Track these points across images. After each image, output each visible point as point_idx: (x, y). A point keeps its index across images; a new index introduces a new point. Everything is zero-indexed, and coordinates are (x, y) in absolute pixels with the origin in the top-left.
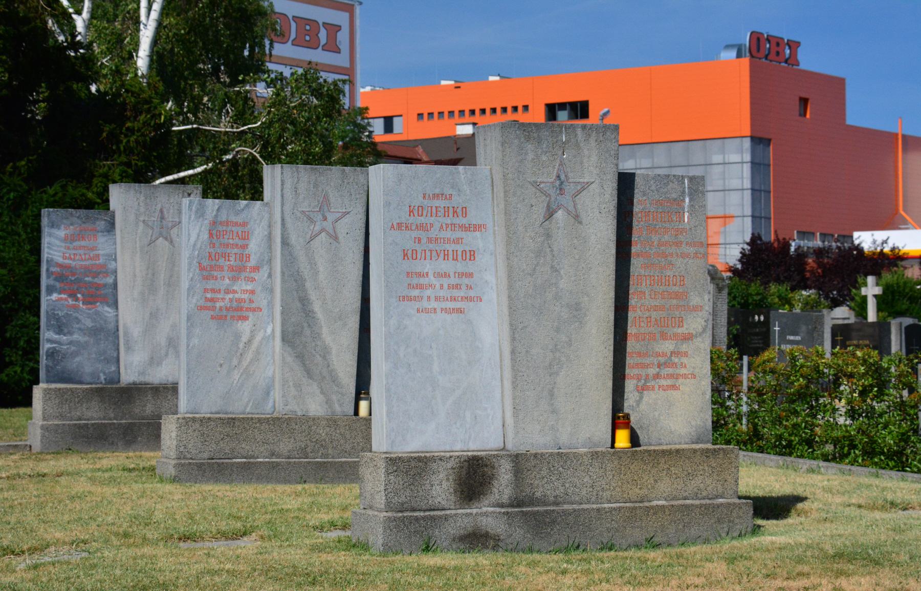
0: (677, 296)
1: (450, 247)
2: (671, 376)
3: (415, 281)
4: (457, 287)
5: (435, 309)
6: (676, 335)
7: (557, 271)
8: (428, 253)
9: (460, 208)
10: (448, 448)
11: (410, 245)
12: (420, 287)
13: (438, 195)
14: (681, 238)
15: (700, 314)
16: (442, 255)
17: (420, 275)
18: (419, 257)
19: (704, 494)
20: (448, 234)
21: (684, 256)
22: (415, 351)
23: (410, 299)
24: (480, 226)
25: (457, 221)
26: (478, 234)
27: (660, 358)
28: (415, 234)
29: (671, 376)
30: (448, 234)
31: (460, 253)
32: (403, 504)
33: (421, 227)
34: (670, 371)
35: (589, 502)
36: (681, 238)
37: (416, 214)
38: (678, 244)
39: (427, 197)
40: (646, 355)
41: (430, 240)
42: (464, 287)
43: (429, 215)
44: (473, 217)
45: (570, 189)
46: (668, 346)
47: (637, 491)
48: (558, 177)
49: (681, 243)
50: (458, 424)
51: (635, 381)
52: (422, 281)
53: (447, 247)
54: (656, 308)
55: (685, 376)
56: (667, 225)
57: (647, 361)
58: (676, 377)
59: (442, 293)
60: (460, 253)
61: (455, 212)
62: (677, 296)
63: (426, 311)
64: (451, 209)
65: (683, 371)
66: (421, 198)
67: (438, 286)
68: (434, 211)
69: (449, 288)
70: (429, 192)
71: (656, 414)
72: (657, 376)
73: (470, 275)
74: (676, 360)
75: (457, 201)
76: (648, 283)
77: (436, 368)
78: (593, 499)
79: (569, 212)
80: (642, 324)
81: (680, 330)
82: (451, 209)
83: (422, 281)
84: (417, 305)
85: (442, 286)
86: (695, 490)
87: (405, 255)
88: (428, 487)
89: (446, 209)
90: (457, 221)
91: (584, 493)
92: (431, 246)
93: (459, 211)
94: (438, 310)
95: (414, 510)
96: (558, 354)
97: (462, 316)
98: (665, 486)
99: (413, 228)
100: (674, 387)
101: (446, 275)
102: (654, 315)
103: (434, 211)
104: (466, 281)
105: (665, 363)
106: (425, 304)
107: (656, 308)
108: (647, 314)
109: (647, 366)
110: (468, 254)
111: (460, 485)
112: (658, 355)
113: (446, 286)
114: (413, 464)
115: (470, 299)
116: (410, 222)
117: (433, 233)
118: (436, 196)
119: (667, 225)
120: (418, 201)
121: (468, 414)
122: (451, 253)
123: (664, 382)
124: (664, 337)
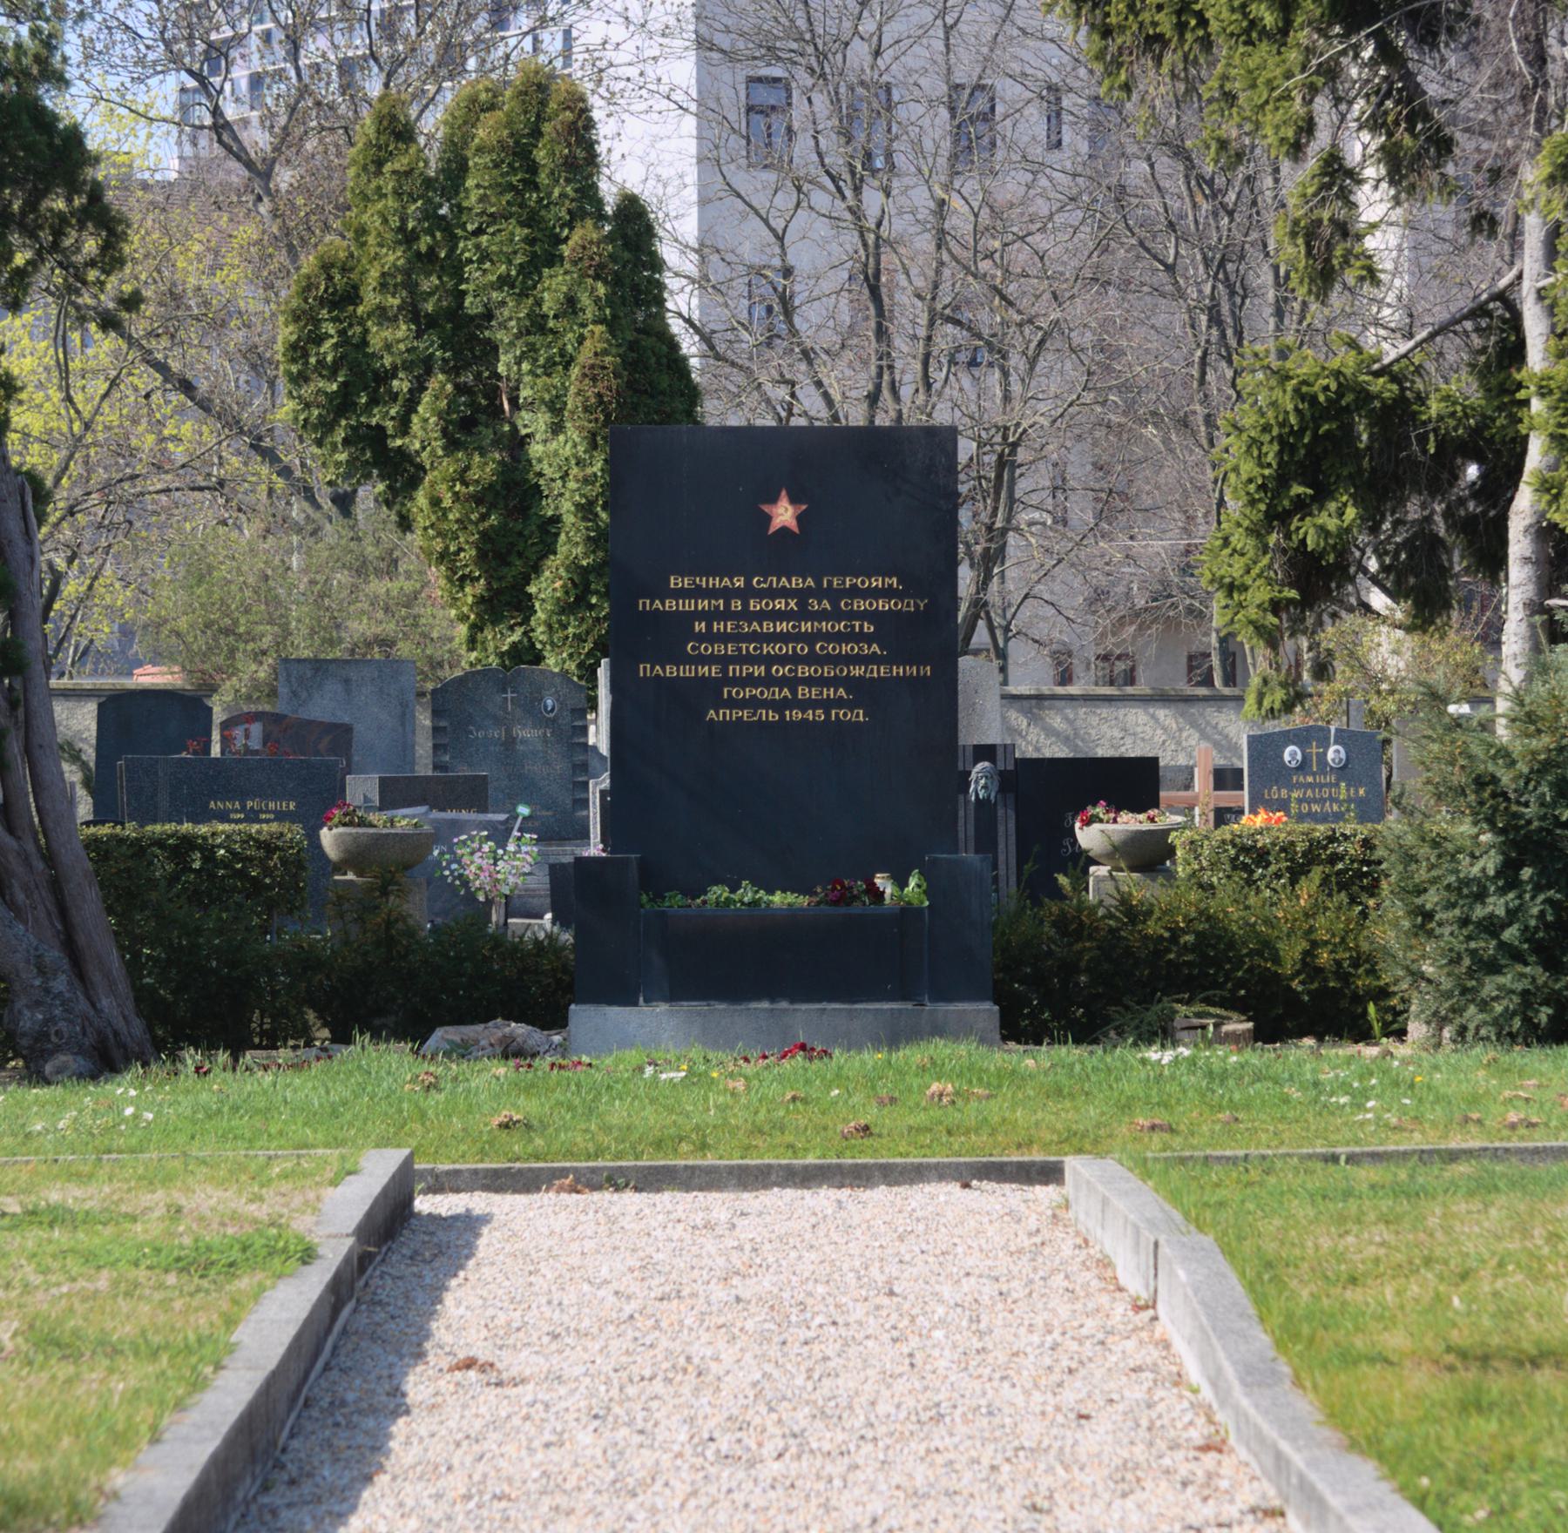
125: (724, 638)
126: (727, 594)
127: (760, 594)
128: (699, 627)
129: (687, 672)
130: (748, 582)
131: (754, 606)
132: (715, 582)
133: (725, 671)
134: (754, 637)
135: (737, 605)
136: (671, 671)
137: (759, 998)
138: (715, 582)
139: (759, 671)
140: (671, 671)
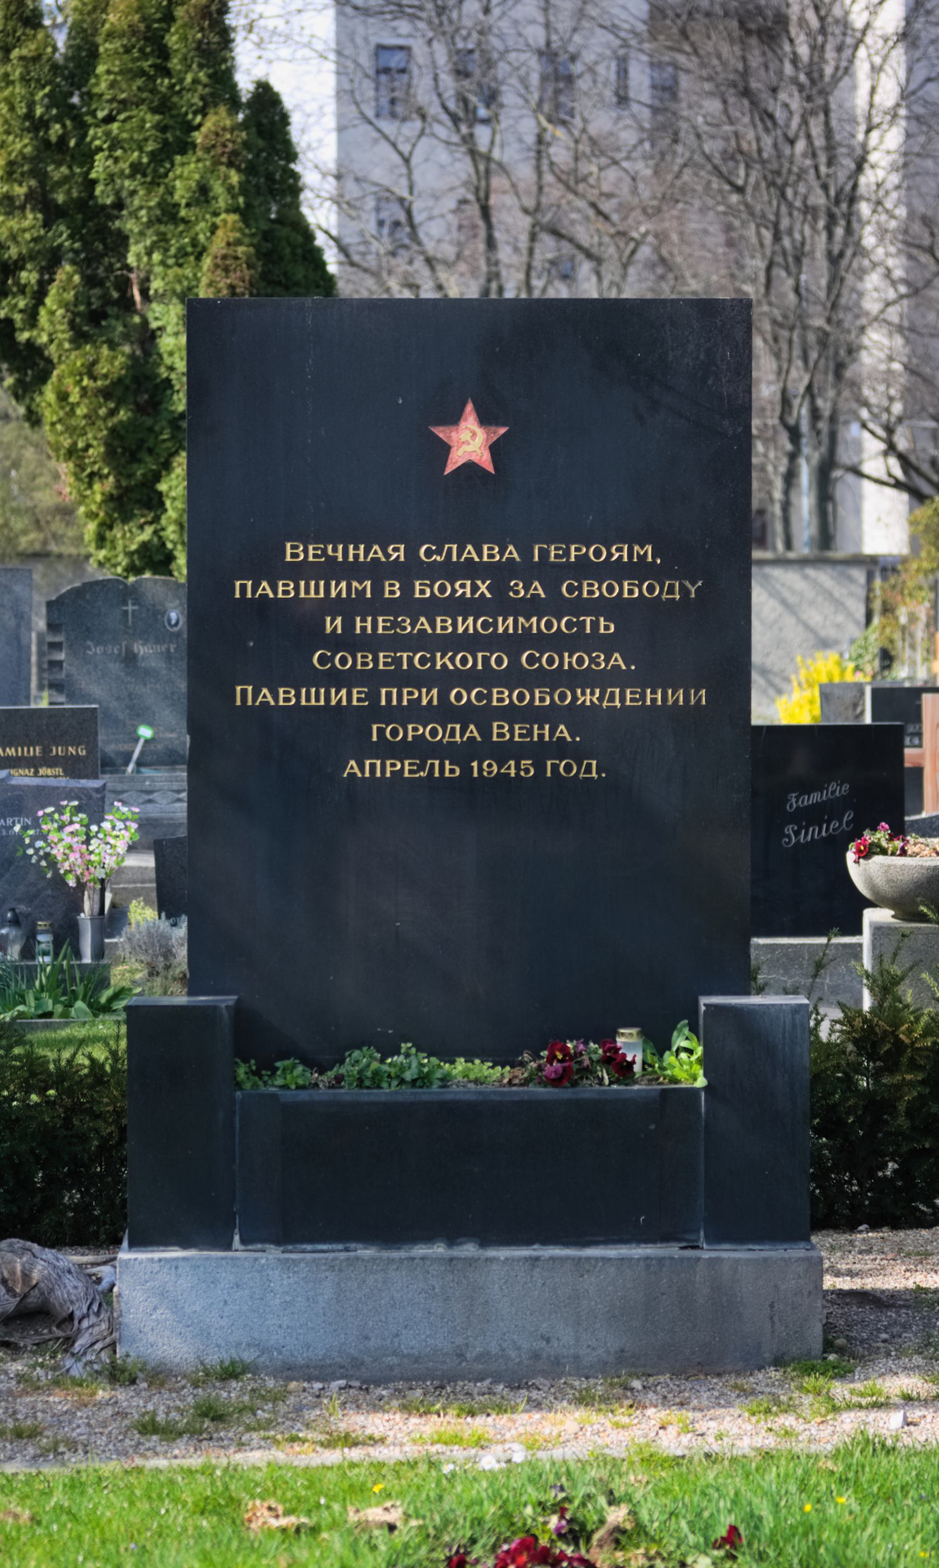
125: (372, 643)
126: (377, 572)
127: (431, 572)
129: (313, 698)
130: (412, 552)
131: (421, 590)
132: (358, 553)
134: (421, 641)
135: (392, 589)
136: (286, 696)
137: (429, 1238)
138: (358, 553)
139: (429, 696)
140: (286, 696)
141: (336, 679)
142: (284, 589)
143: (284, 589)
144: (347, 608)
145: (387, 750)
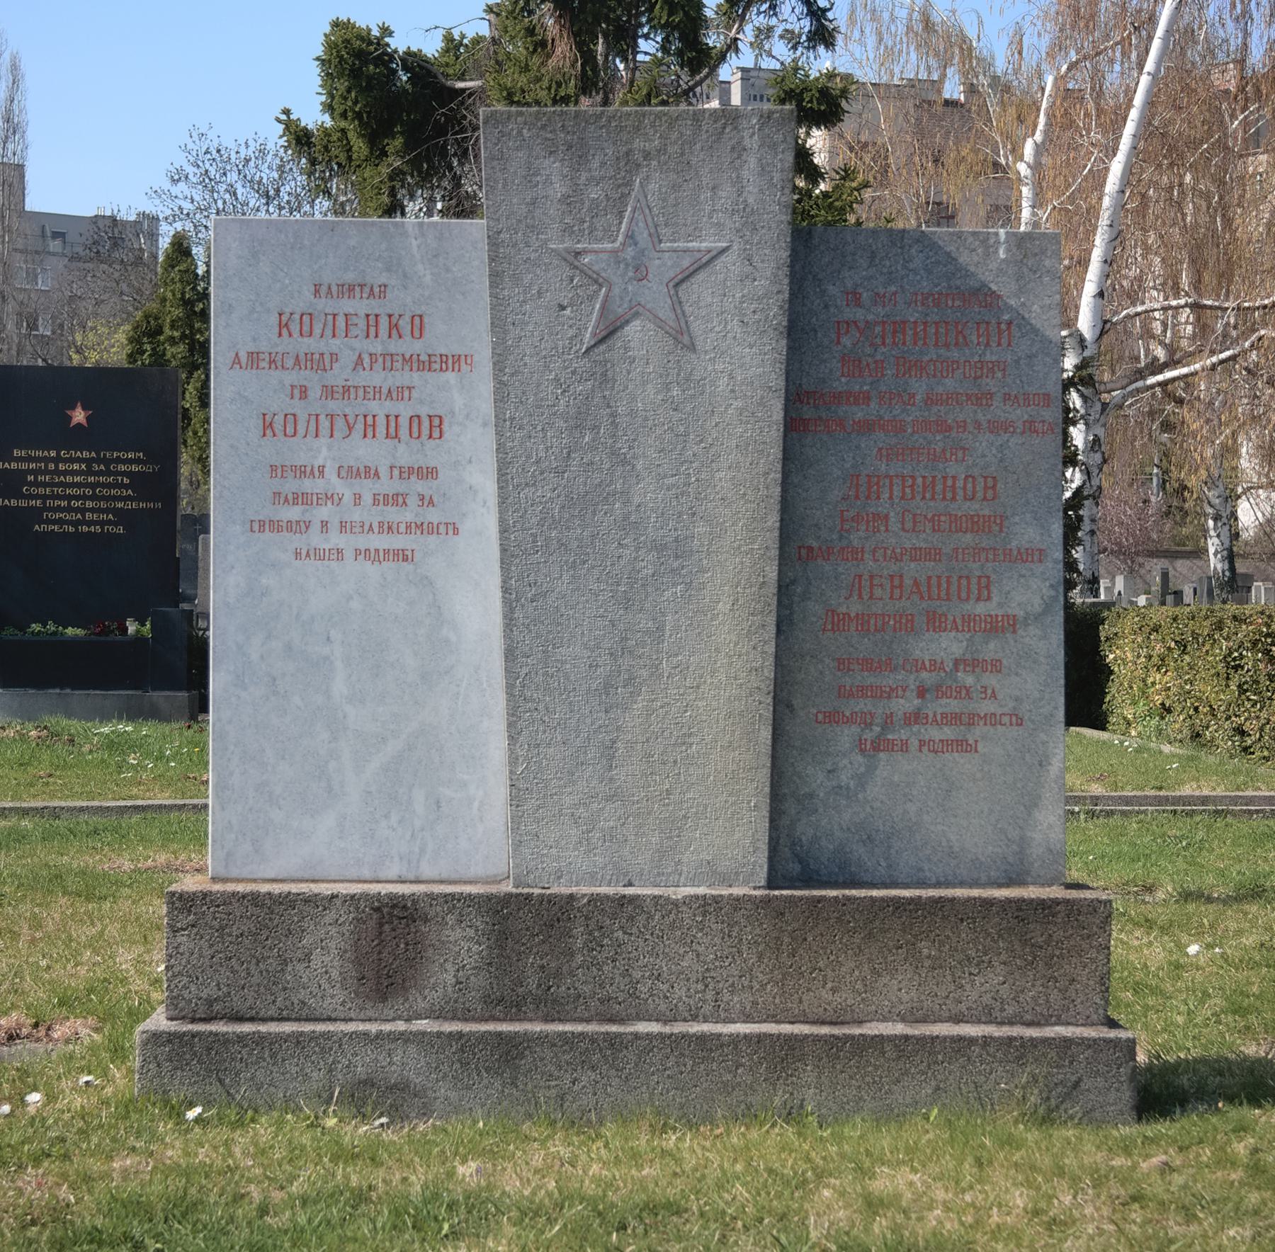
0: (976, 524)
1: (379, 408)
2: (954, 719)
3: (291, 485)
4: (398, 500)
5: (340, 551)
6: (969, 621)
7: (624, 462)
8: (325, 423)
9: (407, 318)
10: (367, 874)
11: (279, 404)
12: (300, 498)
13: (351, 289)
14: (990, 384)
15: (1038, 568)
16: (360, 426)
17: (302, 472)
18: (301, 431)
19: (1010, 1010)
20: (377, 378)
21: (997, 427)
22: (289, 648)
23: (275, 526)
24: (457, 359)
25: (395, 346)
26: (451, 376)
27: (924, 675)
28: (291, 377)
29: (954, 719)
30: (377, 378)
31: (404, 422)
32: (210, 1002)
33: (316, 362)
34: (953, 705)
35: (695, 1018)
36: (990, 384)
37: (296, 334)
38: (982, 399)
39: (324, 290)
40: (889, 665)
41: (329, 392)
42: (413, 501)
43: (329, 332)
44: (439, 339)
45: (663, 266)
46: (949, 646)
47: (825, 994)
48: (630, 236)
49: (991, 395)
50: (394, 819)
51: (855, 729)
52: (308, 485)
53: (375, 407)
54: (916, 555)
55: (992, 720)
56: (955, 354)
57: (889, 680)
58: (971, 720)
59: (356, 515)
60: (404, 422)
61: (394, 327)
62: (976, 524)
63: (319, 554)
64: (384, 322)
65: (987, 707)
66: (308, 293)
67: (348, 497)
68: (341, 322)
69: (376, 502)
70: (328, 278)
71: (912, 808)
72: (915, 718)
73: (429, 473)
74: (969, 680)
75: (400, 301)
76: (897, 492)
77: (339, 687)
78: (707, 1009)
79: (660, 323)
80: (878, 592)
81: (981, 609)
82: (384, 322)
83: (308, 485)
84: (296, 541)
85: (358, 498)
86: (987, 999)
87: (267, 427)
88: (273, 964)
89: (372, 321)
90: (395, 346)
91: (680, 992)
92: (333, 406)
93: (404, 324)
94: (349, 554)
95: (240, 1019)
96: (626, 662)
97: (408, 567)
98: (901, 987)
99: (289, 363)
100: (961, 745)
101: (370, 473)
102: (911, 570)
103: (341, 322)
104: (418, 486)
105: (938, 688)
106: (315, 539)
107: (916, 555)
108: (894, 568)
109: (890, 693)
110: (426, 424)
111: (357, 962)
112: (919, 666)
113: (367, 498)
114: (237, 909)
115: (432, 529)
116: (279, 349)
117: (339, 375)
118: (349, 290)
119: (955, 354)
120: (303, 300)
121: (419, 796)
122: (381, 421)
123: (935, 734)
124: (936, 622)
125: (45, 485)
126: (47, 460)
127: (65, 461)
128: (31, 478)
129: (23, 503)
130: (58, 454)
131: (61, 467)
132: (39, 453)
133: (44, 503)
134: (61, 484)
135: (52, 466)
136: (14, 503)
137: (54, 687)
138: (39, 453)
139: (64, 503)
140: (14, 503)
141: (31, 497)
142: (14, 466)
143: (14, 466)
144: (35, 472)
145: (49, 522)
